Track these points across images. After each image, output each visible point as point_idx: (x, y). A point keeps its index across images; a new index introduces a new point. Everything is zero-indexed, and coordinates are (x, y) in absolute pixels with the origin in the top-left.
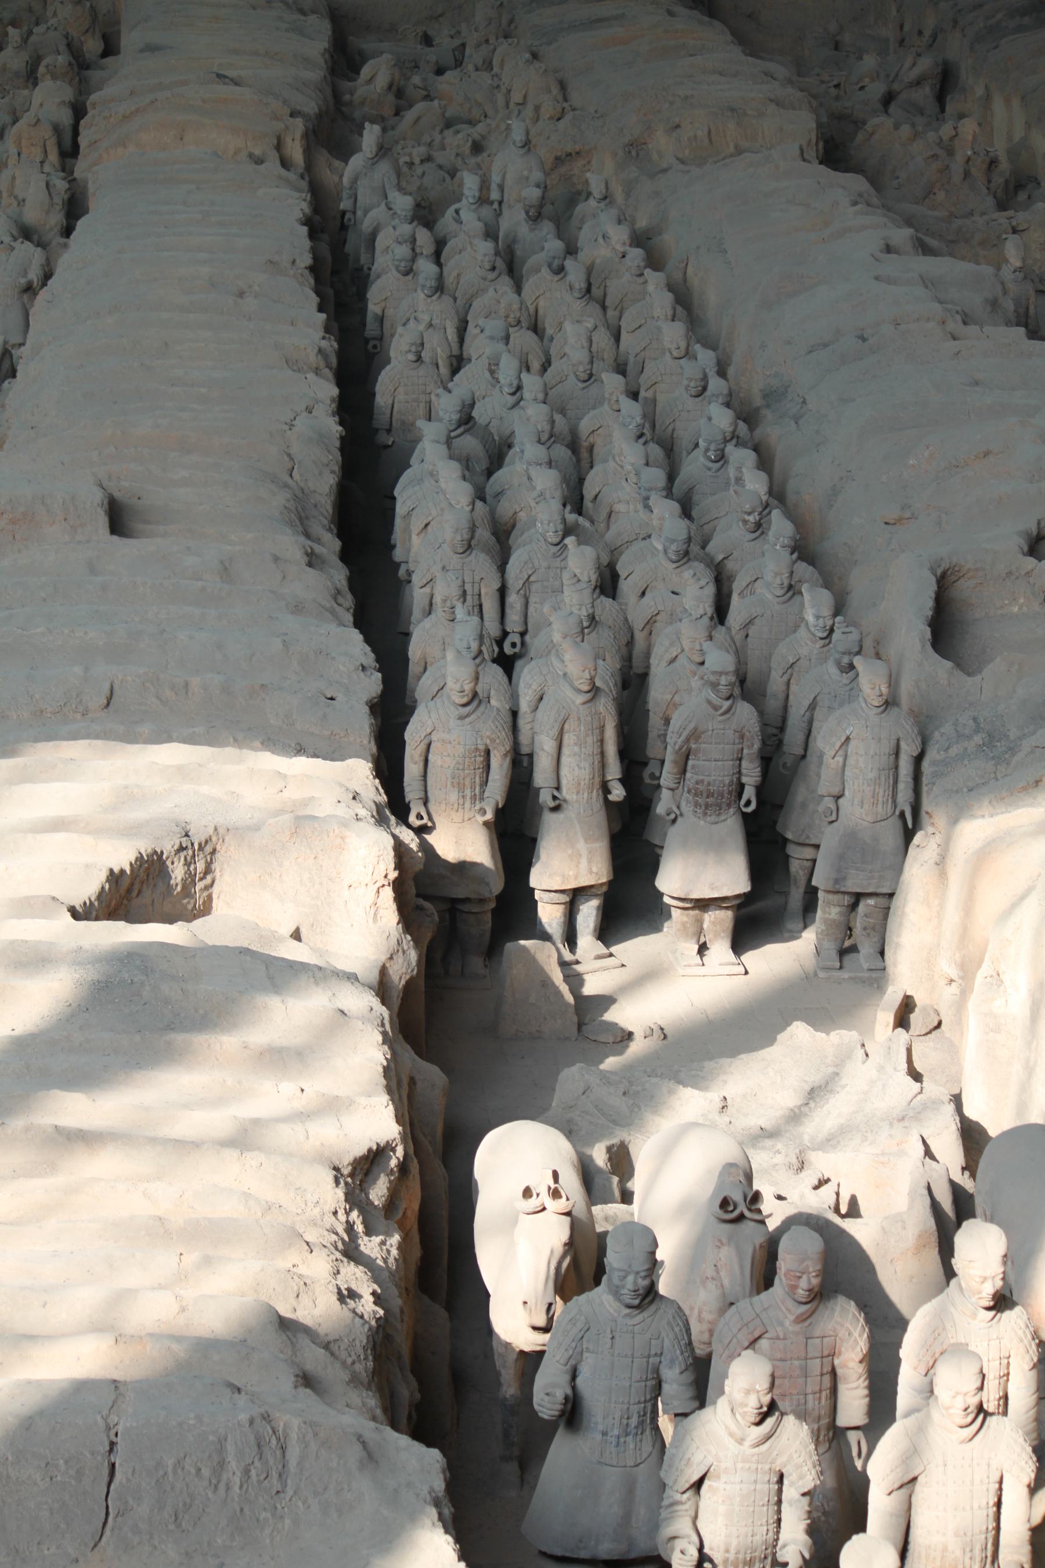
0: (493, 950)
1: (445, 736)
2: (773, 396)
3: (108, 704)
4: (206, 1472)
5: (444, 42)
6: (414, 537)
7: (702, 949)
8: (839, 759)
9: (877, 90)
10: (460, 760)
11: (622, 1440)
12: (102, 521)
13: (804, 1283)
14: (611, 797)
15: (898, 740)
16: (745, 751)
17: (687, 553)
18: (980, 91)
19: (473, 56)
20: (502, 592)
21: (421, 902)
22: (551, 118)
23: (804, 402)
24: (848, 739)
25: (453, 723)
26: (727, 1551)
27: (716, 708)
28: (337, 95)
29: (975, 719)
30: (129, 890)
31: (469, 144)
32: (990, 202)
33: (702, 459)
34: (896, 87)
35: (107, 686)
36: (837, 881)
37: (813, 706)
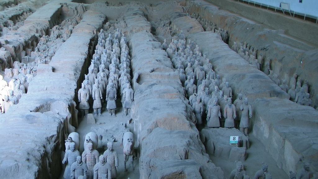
4: (10, 170)
5: (118, 20)
9: (163, 24)
12: (52, 71)
13: (90, 149)
25: (82, 90)
28: (103, 26)
30: (39, 109)
36: (125, 107)
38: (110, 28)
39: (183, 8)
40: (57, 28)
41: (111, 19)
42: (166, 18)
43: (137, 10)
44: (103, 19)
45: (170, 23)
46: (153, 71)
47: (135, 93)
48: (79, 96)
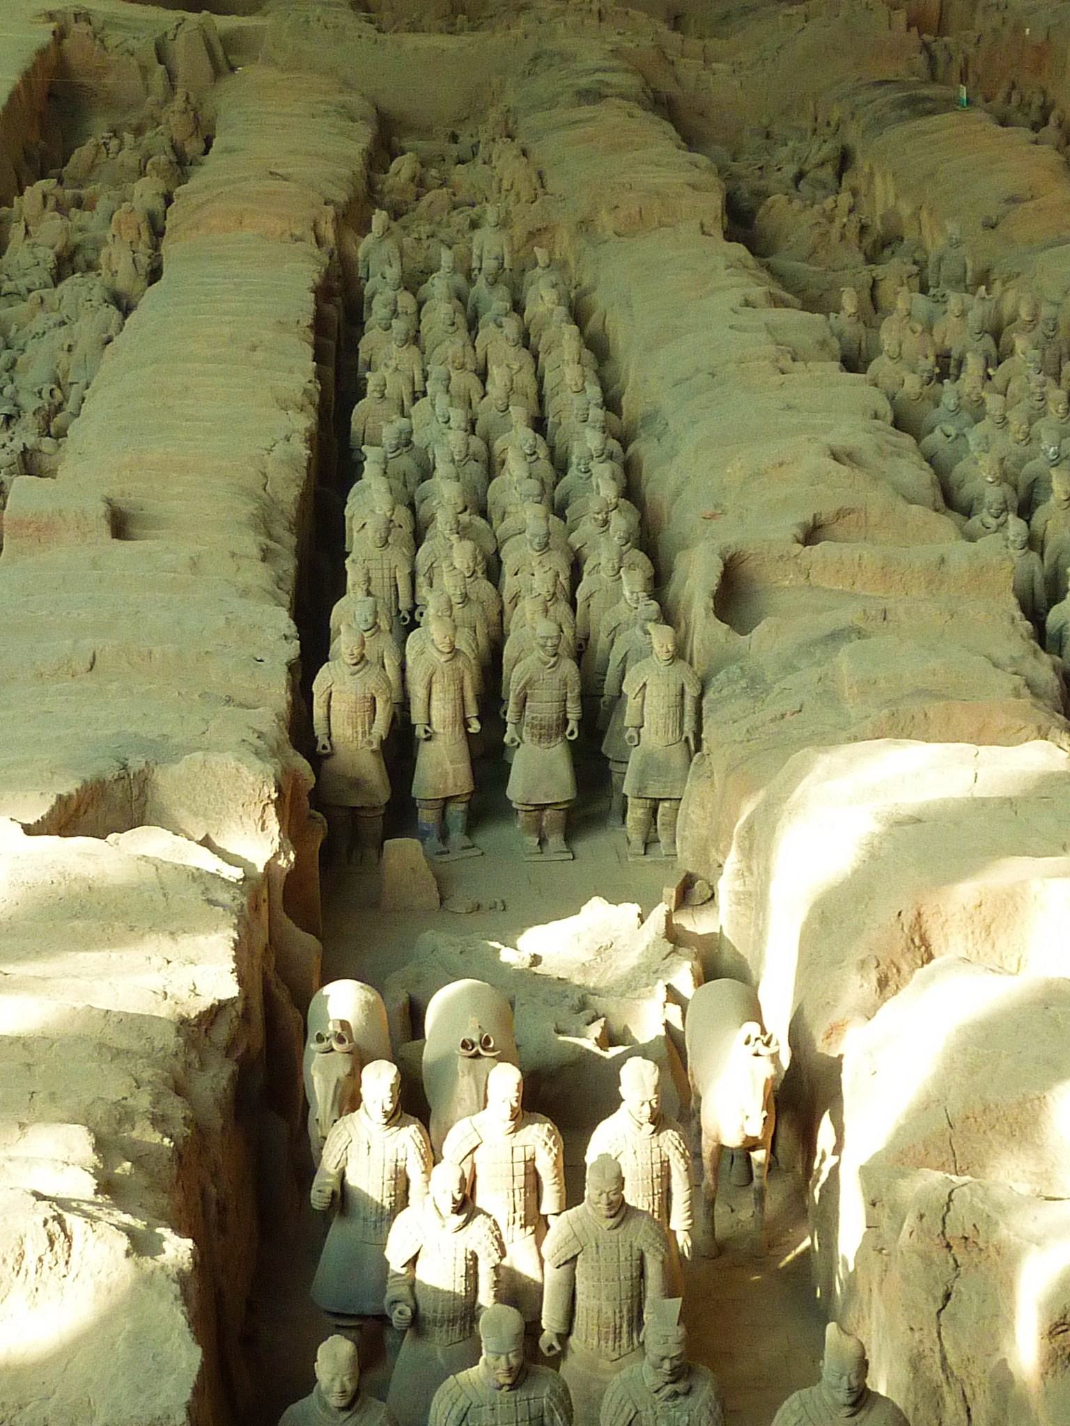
0: (381, 847)
1: (342, 688)
2: (649, 419)
3: (92, 667)
4: (10, 1261)
5: (466, 140)
6: (355, 534)
7: (542, 842)
8: (639, 699)
9: (791, 170)
10: (353, 705)
11: (378, 1224)
12: (105, 529)
14: (471, 730)
15: (683, 685)
16: (569, 695)
17: (547, 544)
18: (866, 169)
19: (482, 152)
20: (413, 576)
21: (313, 812)
22: (527, 201)
23: (667, 424)
24: (645, 685)
25: (347, 678)
26: (435, 1311)
27: (545, 663)
28: (371, 184)
29: (741, 668)
30: (77, 810)
31: (468, 222)
32: (861, 257)
33: (576, 472)
34: (807, 167)
35: (90, 655)
36: (639, 790)
37: (624, 660)
38: (418, 198)
39: (926, 47)
40: (45, 197)
41: (411, 129)
42: (807, 124)
43: (606, 64)
44: (361, 138)
45: (844, 161)
46: (812, 534)
47: (711, 695)
48: (318, 711)
